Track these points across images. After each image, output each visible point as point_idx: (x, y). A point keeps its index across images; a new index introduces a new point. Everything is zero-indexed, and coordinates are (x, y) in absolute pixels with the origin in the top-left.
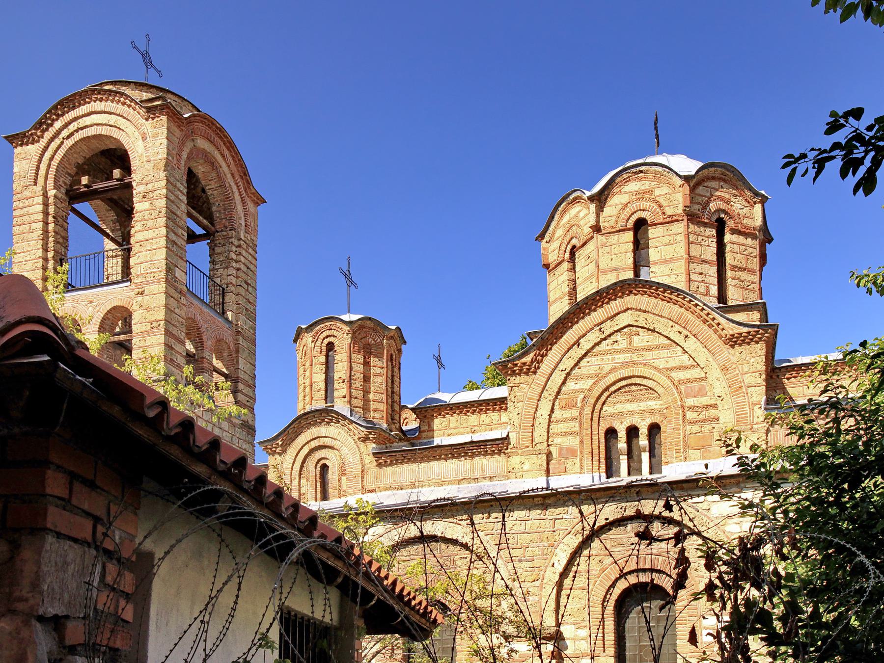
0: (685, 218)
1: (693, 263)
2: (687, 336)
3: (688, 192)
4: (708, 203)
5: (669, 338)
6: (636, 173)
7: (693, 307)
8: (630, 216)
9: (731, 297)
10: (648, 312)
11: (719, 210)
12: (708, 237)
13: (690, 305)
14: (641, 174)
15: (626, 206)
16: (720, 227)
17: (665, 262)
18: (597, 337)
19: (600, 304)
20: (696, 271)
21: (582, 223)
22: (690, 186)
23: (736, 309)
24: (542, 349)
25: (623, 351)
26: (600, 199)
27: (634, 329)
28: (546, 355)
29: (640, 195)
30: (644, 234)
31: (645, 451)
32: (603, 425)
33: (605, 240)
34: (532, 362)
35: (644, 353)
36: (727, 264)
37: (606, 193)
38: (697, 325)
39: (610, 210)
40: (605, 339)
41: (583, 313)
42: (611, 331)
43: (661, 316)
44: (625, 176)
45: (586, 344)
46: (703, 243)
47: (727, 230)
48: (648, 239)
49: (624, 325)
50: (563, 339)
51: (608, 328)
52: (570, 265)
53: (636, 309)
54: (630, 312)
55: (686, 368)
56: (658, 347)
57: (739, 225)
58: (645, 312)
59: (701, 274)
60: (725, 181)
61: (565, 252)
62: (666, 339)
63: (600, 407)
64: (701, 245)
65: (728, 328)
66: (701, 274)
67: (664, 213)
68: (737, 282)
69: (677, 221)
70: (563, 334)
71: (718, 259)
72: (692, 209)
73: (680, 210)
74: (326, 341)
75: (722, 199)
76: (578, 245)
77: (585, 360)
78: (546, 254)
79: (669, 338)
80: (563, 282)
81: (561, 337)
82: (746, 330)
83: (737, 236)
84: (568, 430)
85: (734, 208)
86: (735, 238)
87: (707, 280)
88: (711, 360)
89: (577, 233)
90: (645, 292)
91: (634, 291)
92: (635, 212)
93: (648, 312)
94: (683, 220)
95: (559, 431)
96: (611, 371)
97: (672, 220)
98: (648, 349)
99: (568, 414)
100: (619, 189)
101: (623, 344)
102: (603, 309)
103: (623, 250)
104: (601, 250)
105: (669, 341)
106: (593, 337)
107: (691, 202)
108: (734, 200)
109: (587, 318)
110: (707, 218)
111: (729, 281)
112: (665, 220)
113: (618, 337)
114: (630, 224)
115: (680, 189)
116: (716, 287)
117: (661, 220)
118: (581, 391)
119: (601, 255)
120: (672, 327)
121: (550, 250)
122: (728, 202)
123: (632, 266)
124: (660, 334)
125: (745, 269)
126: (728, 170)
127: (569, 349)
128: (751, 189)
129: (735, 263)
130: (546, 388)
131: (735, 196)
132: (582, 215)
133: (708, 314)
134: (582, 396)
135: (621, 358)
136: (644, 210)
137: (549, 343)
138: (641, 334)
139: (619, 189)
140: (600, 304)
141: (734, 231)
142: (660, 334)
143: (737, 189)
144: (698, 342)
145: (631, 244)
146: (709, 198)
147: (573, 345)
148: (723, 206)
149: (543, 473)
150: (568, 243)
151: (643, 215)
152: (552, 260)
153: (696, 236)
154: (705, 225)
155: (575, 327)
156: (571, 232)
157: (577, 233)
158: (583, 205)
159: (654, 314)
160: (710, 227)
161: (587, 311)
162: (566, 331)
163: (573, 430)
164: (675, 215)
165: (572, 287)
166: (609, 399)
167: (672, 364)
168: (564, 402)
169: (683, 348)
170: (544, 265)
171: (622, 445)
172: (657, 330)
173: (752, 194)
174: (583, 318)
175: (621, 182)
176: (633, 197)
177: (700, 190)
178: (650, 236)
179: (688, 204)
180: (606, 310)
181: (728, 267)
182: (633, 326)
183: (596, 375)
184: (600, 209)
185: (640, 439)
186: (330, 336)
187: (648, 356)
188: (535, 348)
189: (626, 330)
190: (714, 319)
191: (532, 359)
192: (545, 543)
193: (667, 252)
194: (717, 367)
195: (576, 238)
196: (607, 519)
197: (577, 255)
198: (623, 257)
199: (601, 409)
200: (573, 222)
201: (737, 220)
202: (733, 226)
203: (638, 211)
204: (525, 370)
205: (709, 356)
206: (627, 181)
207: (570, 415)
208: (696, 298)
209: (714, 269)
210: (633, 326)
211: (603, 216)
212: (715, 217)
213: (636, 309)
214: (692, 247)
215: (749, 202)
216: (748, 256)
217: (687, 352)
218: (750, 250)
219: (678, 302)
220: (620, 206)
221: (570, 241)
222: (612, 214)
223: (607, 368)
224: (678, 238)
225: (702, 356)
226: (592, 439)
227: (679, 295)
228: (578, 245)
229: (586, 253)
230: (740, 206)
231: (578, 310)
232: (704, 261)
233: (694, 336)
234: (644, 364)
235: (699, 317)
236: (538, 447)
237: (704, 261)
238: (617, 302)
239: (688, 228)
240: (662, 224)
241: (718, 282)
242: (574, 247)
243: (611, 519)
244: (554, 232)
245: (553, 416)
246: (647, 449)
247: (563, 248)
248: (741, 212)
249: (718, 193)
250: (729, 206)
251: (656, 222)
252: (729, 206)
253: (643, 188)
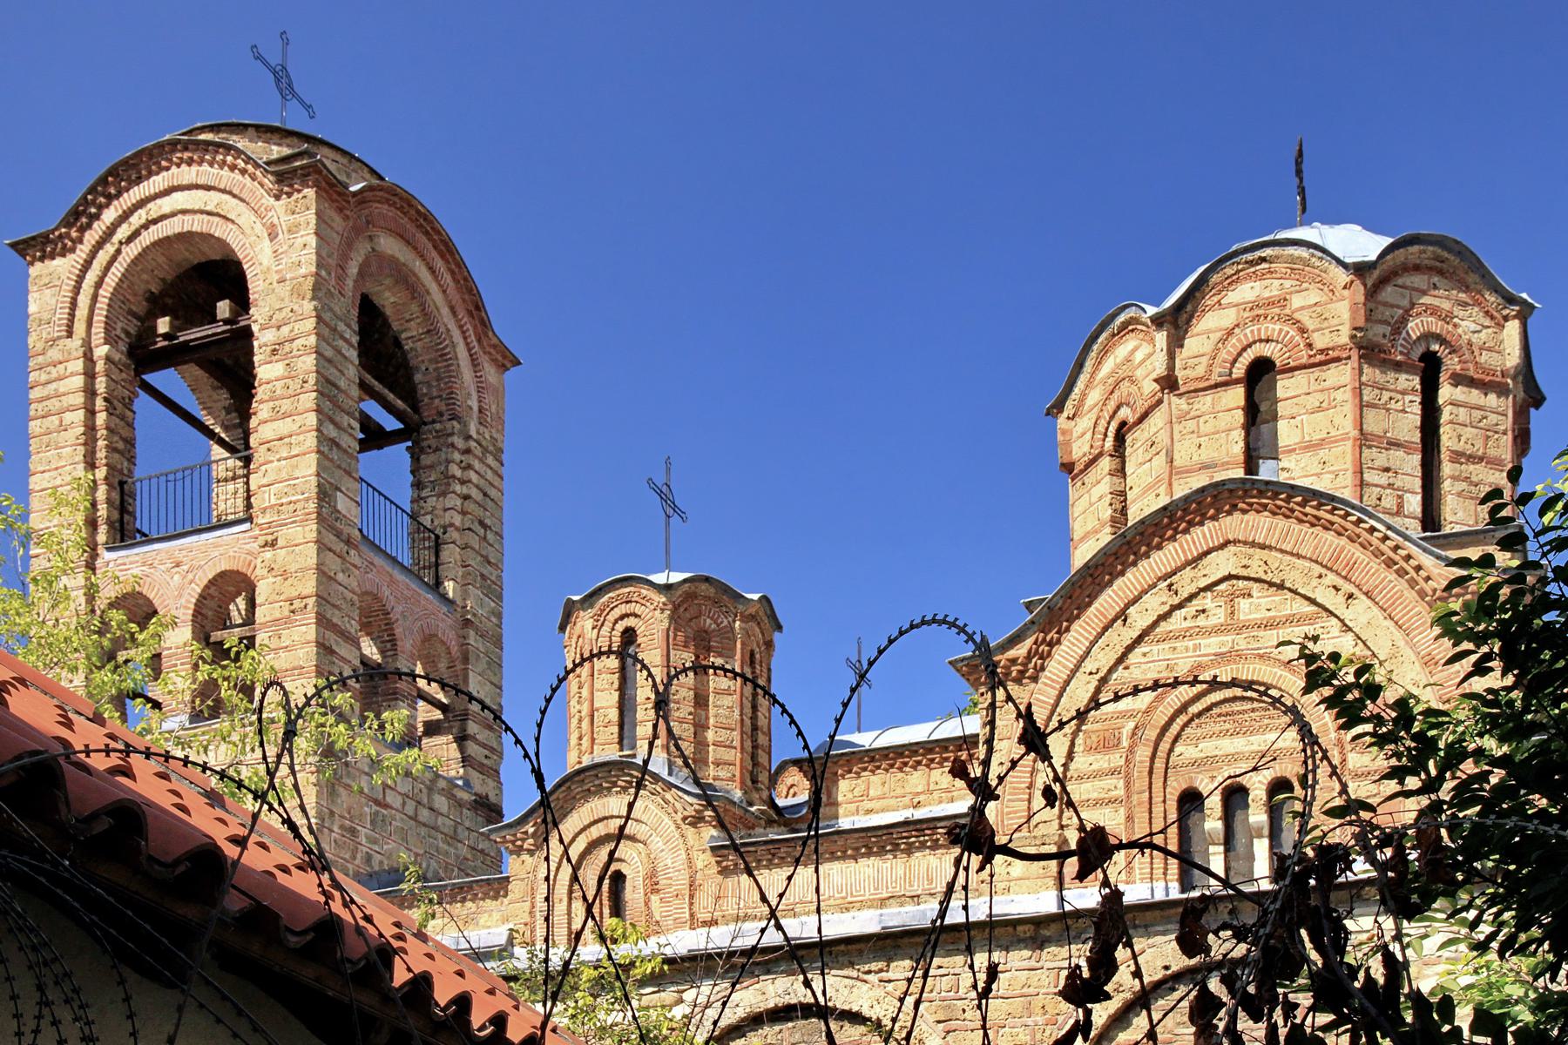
0: (1355, 354)
1: (1370, 447)
2: (1350, 596)
3: (1362, 299)
4: (1404, 321)
5: (1313, 602)
6: (1251, 263)
7: (1365, 535)
8: (1240, 354)
9: (1449, 519)
10: (1270, 548)
11: (1428, 336)
12: (1404, 393)
13: (1358, 531)
14: (1265, 265)
15: (1230, 333)
16: (1430, 370)
17: (1311, 447)
18: (1163, 603)
19: (1170, 533)
20: (1377, 464)
21: (1139, 373)
22: (1365, 285)
23: (1458, 540)
24: (1050, 631)
25: (1218, 630)
26: (1177, 321)
27: (1241, 584)
28: (1059, 642)
29: (1258, 310)
30: (1269, 391)
31: (1260, 836)
32: (1175, 784)
33: (1185, 407)
34: (1029, 657)
35: (1261, 633)
36: (1443, 449)
37: (1189, 307)
38: (1372, 571)
39: (1196, 344)
40: (1180, 606)
41: (1135, 554)
42: (1192, 589)
43: (1298, 556)
44: (1229, 271)
45: (1140, 618)
46: (1392, 405)
47: (1443, 377)
48: (1276, 401)
49: (1219, 575)
50: (1092, 608)
51: (1187, 583)
52: (1115, 463)
53: (1245, 543)
54: (1231, 548)
57: (1471, 366)
58: (1263, 547)
59: (1387, 470)
60: (1441, 272)
61: (1106, 435)
62: (1306, 603)
63: (1168, 746)
64: (1388, 410)
65: (1440, 575)
66: (1387, 470)
67: (1310, 346)
68: (1464, 485)
69: (1338, 360)
70: (1093, 597)
71: (1423, 439)
72: (1370, 334)
73: (1344, 338)
75: (1434, 311)
76: (1131, 420)
77: (1138, 650)
78: (1068, 443)
79: (1313, 602)
80: (1101, 498)
81: (1090, 604)
83: (1465, 389)
84: (1102, 796)
85: (1460, 331)
86: (1460, 393)
87: (1398, 484)
88: (1401, 643)
89: (1129, 394)
90: (1265, 506)
91: (1241, 505)
92: (1250, 346)
93: (1270, 548)
94: (1349, 358)
95: (1083, 797)
97: (1327, 359)
99: (1102, 762)
100: (1216, 299)
102: (1176, 544)
103: (1222, 425)
104: (1177, 428)
105: (1313, 608)
106: (1155, 603)
107: (1367, 320)
108: (1461, 314)
109: (1143, 565)
110: (1401, 353)
111: (1446, 485)
112: (1312, 360)
113: (1207, 601)
114: (1239, 371)
115: (1346, 293)
116: (1419, 497)
117: (1304, 361)
118: (1130, 714)
119: (1177, 436)
120: (1320, 577)
121: (1075, 435)
122: (1447, 318)
123: (1241, 458)
124: (1295, 592)
125: (1481, 459)
126: (1450, 251)
127: (1105, 629)
128: (1497, 289)
129: (1459, 447)
130: (1058, 710)
131: (1464, 304)
132: (1139, 356)
133: (1396, 548)
136: (1267, 341)
137: (1064, 618)
138: (1255, 594)
139: (1216, 299)
140: (1170, 533)
141: (1458, 380)
142: (1295, 592)
143: (1467, 289)
144: (1375, 609)
145: (1240, 413)
146: (1407, 311)
147: (1114, 621)
148: (1436, 326)
149: (1051, 882)
150: (1112, 417)
151: (1266, 350)
152: (1080, 454)
153: (1378, 392)
154: (1398, 367)
156: (1116, 395)
157: (1129, 394)
158: (1141, 335)
159: (1282, 551)
160: (1407, 372)
161: (1144, 549)
162: (1101, 591)
163: (1114, 793)
164: (1333, 349)
165: (1119, 507)
166: (1188, 730)
168: (1094, 738)
169: (1342, 621)
170: (1063, 465)
171: (1213, 823)
172: (1288, 585)
173: (1500, 300)
174: (1134, 564)
175: (1221, 282)
176: (1247, 314)
177: (1388, 293)
178: (1280, 393)
179: (1361, 322)
180: (1182, 547)
181: (1444, 456)
182: (1237, 577)
184: (1176, 342)
185: (1250, 811)
188: (1035, 628)
189: (1222, 587)
190: (1408, 557)
191: (1029, 651)
192: (1038, 1018)
193: (1316, 427)
194: (1413, 658)
195: (1128, 405)
196: (1166, 968)
197: (1129, 439)
198: (1223, 441)
199: (1171, 750)
200: (1121, 374)
201: (1467, 356)
202: (1458, 367)
203: (1255, 342)
204: (1014, 674)
205: (1398, 636)
206: (1234, 280)
207: (1106, 765)
208: (1371, 516)
209: (1416, 458)
210: (1237, 577)
211: (1182, 356)
212: (1419, 351)
213: (1245, 543)
214: (1370, 414)
215: (1492, 318)
216: (1489, 432)
217: (1350, 629)
218: (1493, 418)
219: (1332, 524)
220: (1219, 335)
221: (1115, 412)
222: (1201, 352)
224: (1340, 395)
226: (1150, 813)
227: (1335, 508)
228: (1131, 420)
229: (1146, 435)
230: (1473, 327)
231: (1125, 547)
232: (1394, 444)
233: (1366, 594)
234: (1261, 656)
235: (1378, 553)
236: (1042, 830)
237: (1394, 444)
238: (1205, 528)
239: (1361, 373)
240: (1304, 367)
241: (1424, 487)
242: (1123, 424)
243: (1174, 968)
244: (1084, 395)
245: (1072, 766)
246: (1266, 832)
247: (1101, 429)
248: (1475, 337)
249: (1426, 300)
250: (1450, 328)
251: (1292, 364)
252: (1450, 328)
253: (1267, 294)
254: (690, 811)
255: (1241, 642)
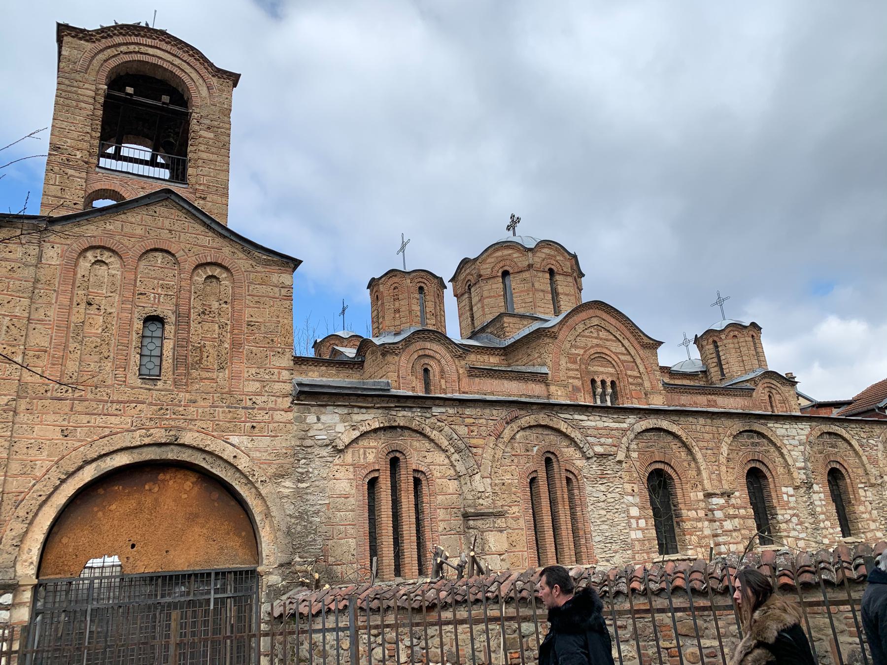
5: (615, 337)
27: (600, 328)
40: (586, 329)
54: (597, 318)
55: (624, 354)
56: (611, 340)
74: (419, 285)
82: (652, 342)
96: (591, 348)
98: (607, 340)
101: (595, 335)
118: (579, 355)
134: (579, 358)
135: (595, 341)
151: (552, 267)
155: (573, 318)
167: (618, 351)
183: (585, 348)
186: (424, 283)
187: (608, 343)
189: (595, 327)
223: (590, 345)
225: (633, 352)
254: (459, 353)
255: (600, 342)
